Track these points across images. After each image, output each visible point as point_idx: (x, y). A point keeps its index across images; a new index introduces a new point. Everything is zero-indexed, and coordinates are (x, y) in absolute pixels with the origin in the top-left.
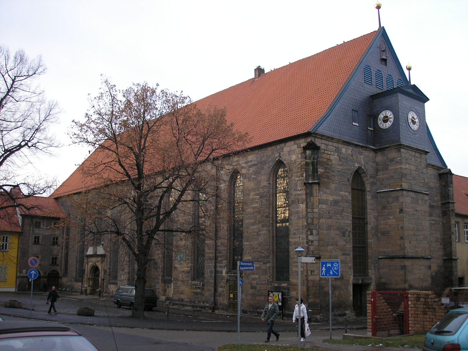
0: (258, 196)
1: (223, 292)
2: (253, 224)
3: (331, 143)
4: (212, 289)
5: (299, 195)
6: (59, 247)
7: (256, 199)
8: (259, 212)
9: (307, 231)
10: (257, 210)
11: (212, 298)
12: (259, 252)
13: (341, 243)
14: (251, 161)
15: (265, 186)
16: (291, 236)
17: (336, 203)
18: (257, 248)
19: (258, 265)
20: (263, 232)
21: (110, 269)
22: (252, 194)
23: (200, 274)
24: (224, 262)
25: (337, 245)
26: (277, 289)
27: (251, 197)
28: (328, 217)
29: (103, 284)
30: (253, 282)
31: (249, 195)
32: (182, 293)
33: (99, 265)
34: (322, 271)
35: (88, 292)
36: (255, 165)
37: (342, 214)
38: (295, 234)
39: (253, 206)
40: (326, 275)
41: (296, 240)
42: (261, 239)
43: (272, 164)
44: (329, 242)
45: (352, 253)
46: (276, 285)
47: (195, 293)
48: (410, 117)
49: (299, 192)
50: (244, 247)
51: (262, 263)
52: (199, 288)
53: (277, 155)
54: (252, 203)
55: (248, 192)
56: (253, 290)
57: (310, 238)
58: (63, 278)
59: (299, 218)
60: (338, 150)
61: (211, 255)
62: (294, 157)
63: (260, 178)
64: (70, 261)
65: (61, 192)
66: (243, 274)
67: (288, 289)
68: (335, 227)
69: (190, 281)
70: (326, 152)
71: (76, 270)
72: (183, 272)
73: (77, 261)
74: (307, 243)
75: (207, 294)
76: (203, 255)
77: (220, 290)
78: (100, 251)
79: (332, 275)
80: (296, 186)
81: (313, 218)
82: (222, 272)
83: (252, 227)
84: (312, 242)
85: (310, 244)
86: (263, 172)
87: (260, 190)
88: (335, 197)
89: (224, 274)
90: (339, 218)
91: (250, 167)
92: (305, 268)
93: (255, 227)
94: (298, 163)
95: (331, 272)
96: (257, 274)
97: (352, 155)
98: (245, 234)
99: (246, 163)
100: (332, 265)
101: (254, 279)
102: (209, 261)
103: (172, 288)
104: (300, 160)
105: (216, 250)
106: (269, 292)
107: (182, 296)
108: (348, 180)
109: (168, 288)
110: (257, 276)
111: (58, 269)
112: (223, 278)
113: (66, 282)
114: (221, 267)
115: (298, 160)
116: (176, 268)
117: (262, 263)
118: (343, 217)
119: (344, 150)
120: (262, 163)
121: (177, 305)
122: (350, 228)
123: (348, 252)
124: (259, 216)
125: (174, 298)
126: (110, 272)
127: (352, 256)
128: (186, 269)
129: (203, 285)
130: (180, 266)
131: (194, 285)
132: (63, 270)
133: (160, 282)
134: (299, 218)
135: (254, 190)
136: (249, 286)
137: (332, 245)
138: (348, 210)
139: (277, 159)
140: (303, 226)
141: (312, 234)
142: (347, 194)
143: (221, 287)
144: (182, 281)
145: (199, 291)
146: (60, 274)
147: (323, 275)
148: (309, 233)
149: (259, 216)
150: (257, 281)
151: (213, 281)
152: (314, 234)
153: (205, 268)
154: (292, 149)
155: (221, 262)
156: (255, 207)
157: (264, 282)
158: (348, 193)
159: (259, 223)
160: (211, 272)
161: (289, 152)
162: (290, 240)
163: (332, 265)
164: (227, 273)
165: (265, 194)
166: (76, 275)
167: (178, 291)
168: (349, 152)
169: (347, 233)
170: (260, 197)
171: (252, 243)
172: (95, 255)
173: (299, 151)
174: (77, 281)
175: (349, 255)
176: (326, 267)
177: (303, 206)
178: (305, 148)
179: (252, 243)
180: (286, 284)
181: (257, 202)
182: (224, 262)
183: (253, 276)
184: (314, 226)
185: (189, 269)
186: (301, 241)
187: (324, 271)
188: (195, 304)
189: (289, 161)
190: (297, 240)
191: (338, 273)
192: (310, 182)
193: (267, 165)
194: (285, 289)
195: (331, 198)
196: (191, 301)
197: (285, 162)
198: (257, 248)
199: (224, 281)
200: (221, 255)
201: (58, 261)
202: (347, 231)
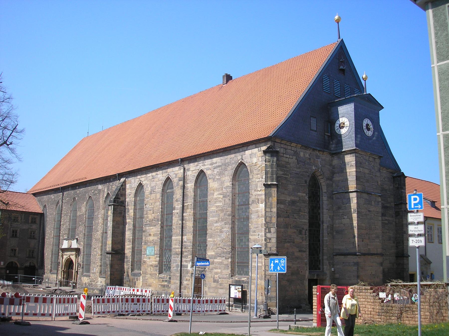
0: (222, 196)
1: (188, 285)
2: (216, 222)
3: (289, 147)
4: (178, 282)
5: (259, 195)
7: (219, 198)
8: (222, 211)
9: (265, 229)
10: (220, 208)
11: (178, 291)
12: (221, 248)
13: (298, 240)
14: (216, 163)
15: (228, 186)
16: (251, 233)
17: (293, 203)
18: (219, 244)
19: (221, 260)
20: (225, 229)
21: (83, 262)
22: (216, 193)
24: (189, 256)
25: (294, 242)
26: (237, 283)
27: (215, 197)
28: (285, 216)
30: (216, 276)
31: (213, 194)
33: (73, 258)
34: (271, 267)
36: (219, 166)
37: (299, 214)
38: (254, 232)
39: (217, 205)
40: (274, 271)
41: (256, 237)
42: (224, 236)
43: (235, 166)
44: (286, 239)
45: (308, 250)
46: (237, 279)
47: (162, 285)
48: (364, 125)
49: (259, 193)
50: (208, 243)
51: (224, 259)
52: (166, 281)
53: (239, 157)
54: (216, 202)
55: (212, 192)
56: (215, 283)
57: (269, 235)
58: (39, 270)
59: (259, 216)
60: (296, 154)
61: (177, 250)
62: (255, 160)
63: (224, 179)
65: (38, 188)
66: (207, 269)
67: (248, 282)
68: (291, 226)
70: (285, 155)
72: (152, 265)
73: (52, 254)
74: (265, 240)
75: (172, 286)
76: (170, 250)
77: (185, 283)
78: (74, 245)
79: (280, 271)
80: (257, 187)
81: (271, 217)
82: (187, 266)
83: (215, 225)
84: (270, 239)
85: (268, 241)
86: (226, 173)
87: (224, 189)
88: (293, 198)
89: (189, 268)
90: (296, 217)
91: (215, 168)
92: (264, 264)
93: (218, 224)
94: (258, 165)
95: (279, 268)
96: (220, 269)
97: (310, 159)
98: (209, 231)
99: (211, 164)
100: (279, 262)
101: (216, 273)
102: (175, 256)
103: (141, 280)
104: (261, 162)
105: (182, 246)
106: (230, 285)
108: (306, 182)
110: (219, 271)
112: (188, 272)
114: (186, 261)
115: (258, 163)
116: (145, 262)
117: (224, 259)
118: (300, 216)
119: (302, 154)
120: (226, 165)
122: (307, 227)
123: (304, 249)
124: (222, 215)
126: (83, 265)
127: (308, 253)
128: (154, 263)
129: (170, 278)
130: (148, 260)
134: (259, 216)
135: (217, 190)
136: (212, 279)
137: (289, 242)
138: (304, 210)
139: (239, 162)
140: (262, 224)
141: (270, 232)
142: (304, 195)
143: (187, 280)
145: (166, 283)
147: (271, 271)
148: (267, 231)
149: (222, 215)
150: (219, 275)
151: (179, 275)
152: (272, 232)
153: (172, 262)
154: (253, 152)
155: (186, 256)
156: (219, 206)
157: (225, 276)
158: (305, 194)
159: (222, 221)
160: (177, 266)
161: (251, 155)
162: (250, 237)
163: (279, 262)
164: (192, 266)
165: (228, 194)
166: (51, 267)
167: (146, 284)
168: (307, 156)
169: (304, 231)
170: (224, 197)
171: (216, 240)
172: (70, 249)
173: (261, 154)
175: (305, 252)
176: (274, 263)
177: (262, 206)
178: (265, 152)
179: (216, 240)
180: (246, 279)
181: (220, 201)
182: (189, 256)
183: (215, 271)
184: (272, 224)
185: (157, 263)
186: (260, 238)
187: (272, 267)
189: (251, 164)
190: (257, 237)
191: (285, 269)
192: (269, 183)
193: (230, 167)
194: (245, 283)
195: (289, 199)
196: (158, 293)
197: (247, 165)
198: (219, 244)
199: (190, 275)
200: (187, 250)
202: (303, 229)
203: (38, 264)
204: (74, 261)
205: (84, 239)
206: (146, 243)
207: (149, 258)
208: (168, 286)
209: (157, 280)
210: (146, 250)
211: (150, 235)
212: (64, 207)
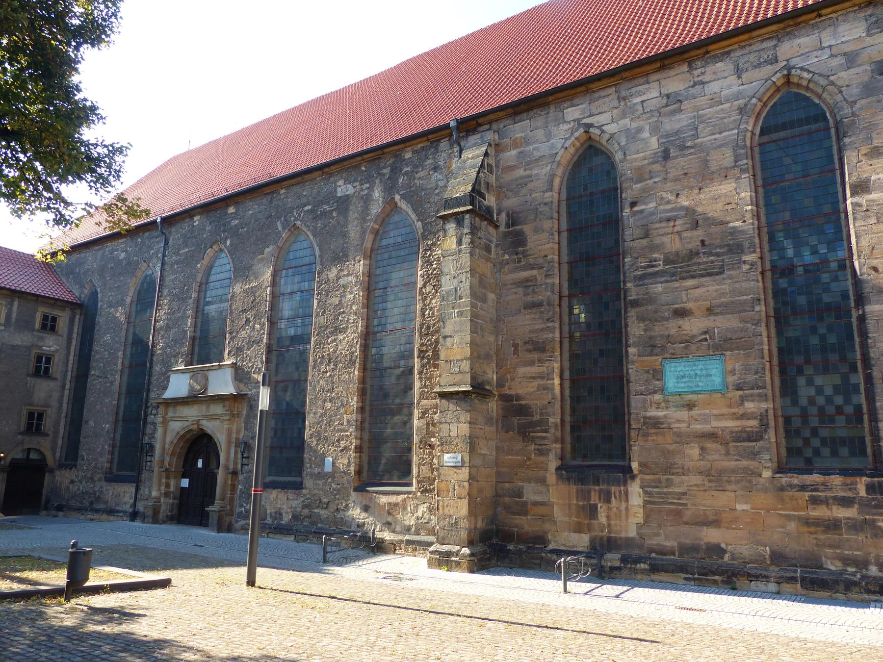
6: (52, 384)
23: (816, 442)
29: (233, 487)
32: (715, 523)
35: (164, 510)
52: (846, 502)
58: (58, 473)
64: (92, 423)
69: (767, 474)
71: (114, 446)
72: (712, 436)
107: (712, 535)
109: (608, 501)
111: (44, 444)
113: (72, 482)
121: (682, 571)
125: (653, 542)
130: (684, 414)
131: (803, 488)
132: (58, 450)
133: (551, 478)
144: (707, 473)
146: (50, 461)
167: (678, 514)
174: (112, 478)
185: (754, 423)
188: (821, 575)
201: (48, 424)
203: (54, 454)
204: (221, 438)
205: (267, 362)
206: (651, 347)
207: (690, 406)
208: (856, 526)
209: (765, 499)
210: (658, 374)
211: (682, 313)
212: (169, 278)
